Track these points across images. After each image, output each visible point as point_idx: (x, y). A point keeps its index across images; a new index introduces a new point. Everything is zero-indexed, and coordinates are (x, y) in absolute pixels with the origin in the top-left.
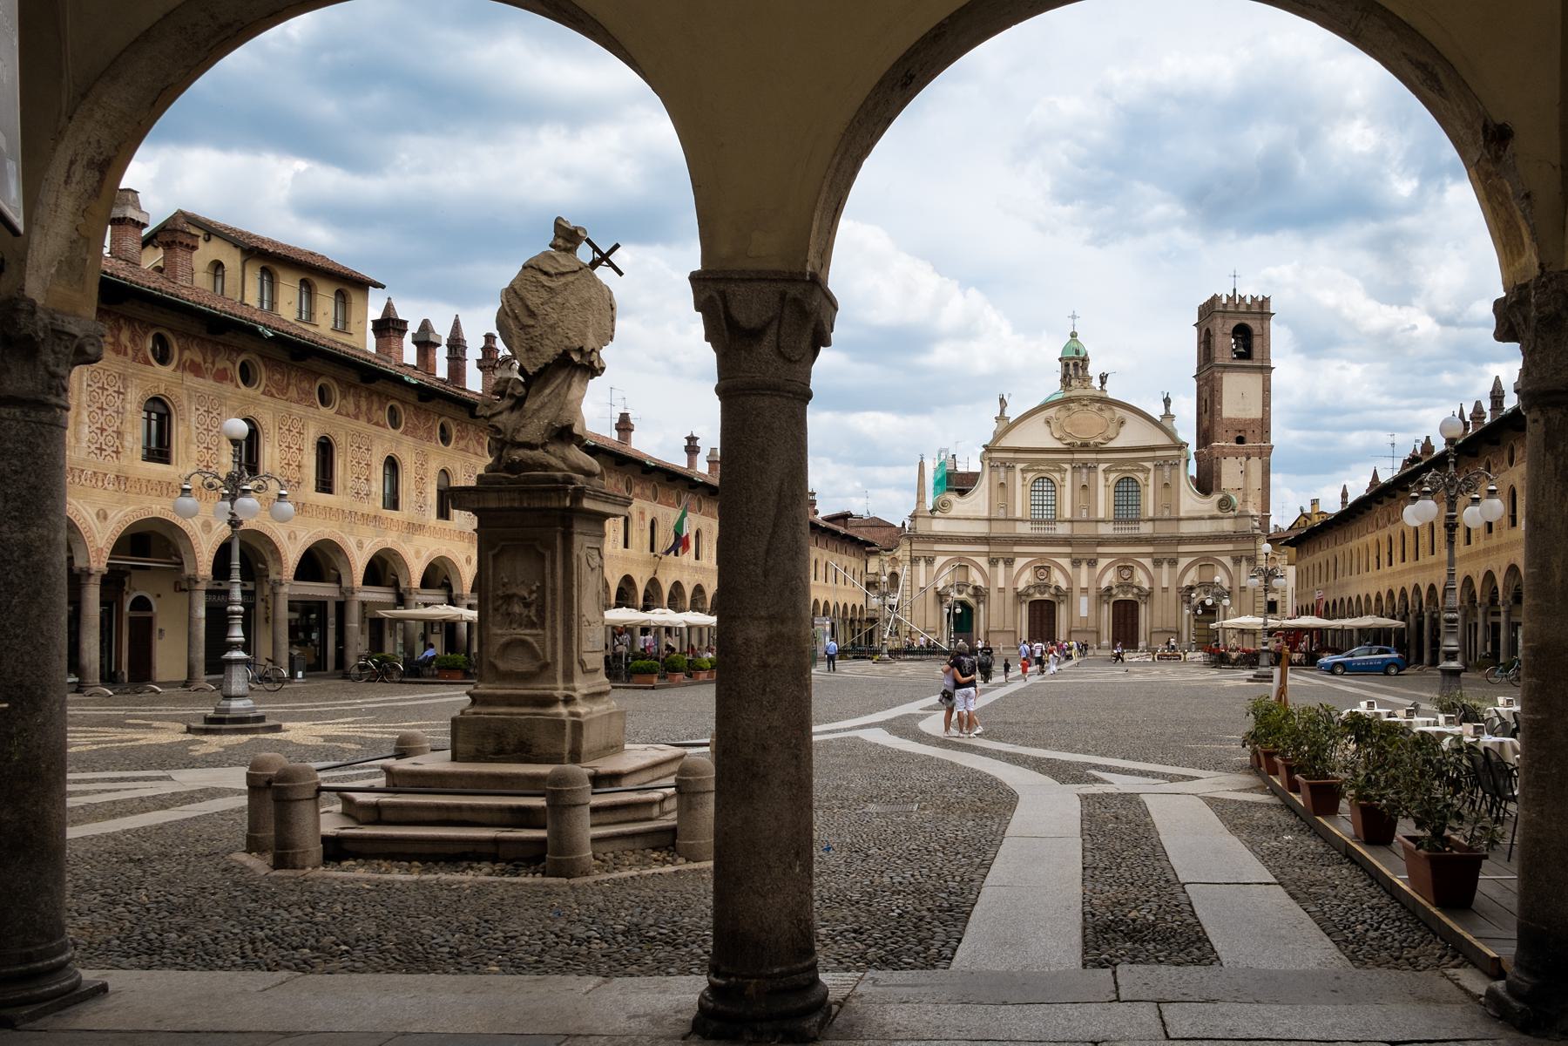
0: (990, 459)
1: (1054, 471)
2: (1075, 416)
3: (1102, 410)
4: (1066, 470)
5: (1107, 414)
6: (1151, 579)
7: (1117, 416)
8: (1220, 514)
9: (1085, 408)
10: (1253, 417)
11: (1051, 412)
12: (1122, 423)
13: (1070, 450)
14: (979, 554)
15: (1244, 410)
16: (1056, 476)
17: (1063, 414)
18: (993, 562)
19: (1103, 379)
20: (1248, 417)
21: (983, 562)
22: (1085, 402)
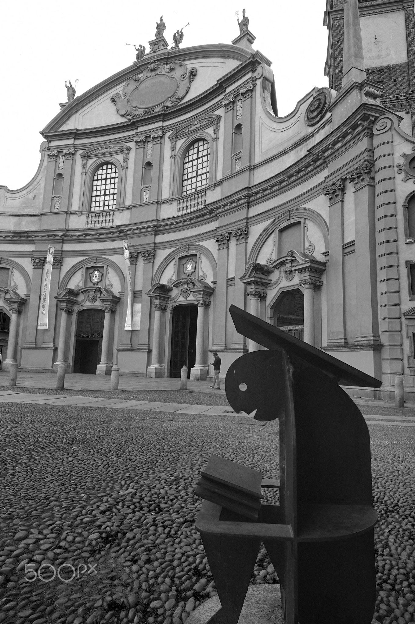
0: (49, 149)
1: (117, 153)
2: (143, 85)
3: (172, 70)
4: (129, 149)
5: (178, 72)
6: (215, 266)
7: (189, 70)
8: (310, 130)
9: (153, 73)
10: (392, 62)
11: (119, 89)
12: (193, 74)
13: (132, 125)
14: (22, 254)
15: (379, 57)
16: (120, 158)
17: (133, 85)
18: (40, 262)
19: (178, 37)
20: (385, 64)
21: (27, 263)
22: (152, 66)
